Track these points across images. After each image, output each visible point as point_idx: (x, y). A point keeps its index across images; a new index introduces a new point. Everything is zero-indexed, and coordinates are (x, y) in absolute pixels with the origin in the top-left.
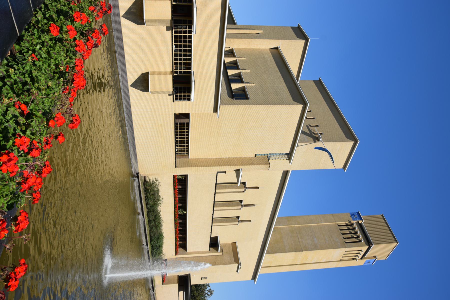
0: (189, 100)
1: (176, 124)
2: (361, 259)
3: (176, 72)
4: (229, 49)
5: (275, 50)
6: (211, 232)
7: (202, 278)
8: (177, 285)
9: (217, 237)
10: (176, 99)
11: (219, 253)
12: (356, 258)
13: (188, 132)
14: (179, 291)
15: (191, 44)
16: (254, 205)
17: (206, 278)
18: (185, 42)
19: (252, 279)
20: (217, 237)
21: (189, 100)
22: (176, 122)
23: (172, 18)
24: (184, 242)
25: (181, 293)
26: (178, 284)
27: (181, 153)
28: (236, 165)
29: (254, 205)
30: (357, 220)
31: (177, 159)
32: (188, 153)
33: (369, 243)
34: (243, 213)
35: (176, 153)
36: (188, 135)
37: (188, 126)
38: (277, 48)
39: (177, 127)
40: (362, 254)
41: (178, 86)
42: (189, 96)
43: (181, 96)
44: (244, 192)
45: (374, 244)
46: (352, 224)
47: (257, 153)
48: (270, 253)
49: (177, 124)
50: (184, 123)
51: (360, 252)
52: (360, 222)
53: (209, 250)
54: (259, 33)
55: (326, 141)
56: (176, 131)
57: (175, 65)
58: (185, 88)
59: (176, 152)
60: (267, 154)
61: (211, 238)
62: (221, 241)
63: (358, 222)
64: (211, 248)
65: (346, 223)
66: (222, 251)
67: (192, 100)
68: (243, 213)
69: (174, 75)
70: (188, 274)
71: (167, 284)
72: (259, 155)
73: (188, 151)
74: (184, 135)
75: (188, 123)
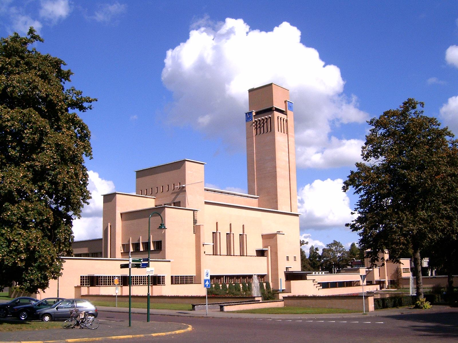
2: (287, 115)
4: (122, 247)
8: (292, 282)
9: (256, 250)
11: (269, 249)
14: (307, 280)
16: (230, 224)
17: (295, 257)
19: (298, 216)
20: (256, 250)
21: (164, 276)
26: (291, 281)
28: (200, 247)
29: (230, 224)
30: (252, 117)
33: (270, 110)
34: (237, 232)
35: (193, 284)
38: (121, 214)
41: (157, 282)
42: (162, 277)
43: (162, 281)
45: (273, 105)
48: (277, 200)
52: (254, 114)
54: (111, 226)
55: (185, 182)
59: (191, 283)
60: (194, 226)
61: (257, 256)
62: (260, 247)
65: (255, 129)
66: (267, 247)
68: (237, 232)
70: (285, 273)
72: (194, 232)
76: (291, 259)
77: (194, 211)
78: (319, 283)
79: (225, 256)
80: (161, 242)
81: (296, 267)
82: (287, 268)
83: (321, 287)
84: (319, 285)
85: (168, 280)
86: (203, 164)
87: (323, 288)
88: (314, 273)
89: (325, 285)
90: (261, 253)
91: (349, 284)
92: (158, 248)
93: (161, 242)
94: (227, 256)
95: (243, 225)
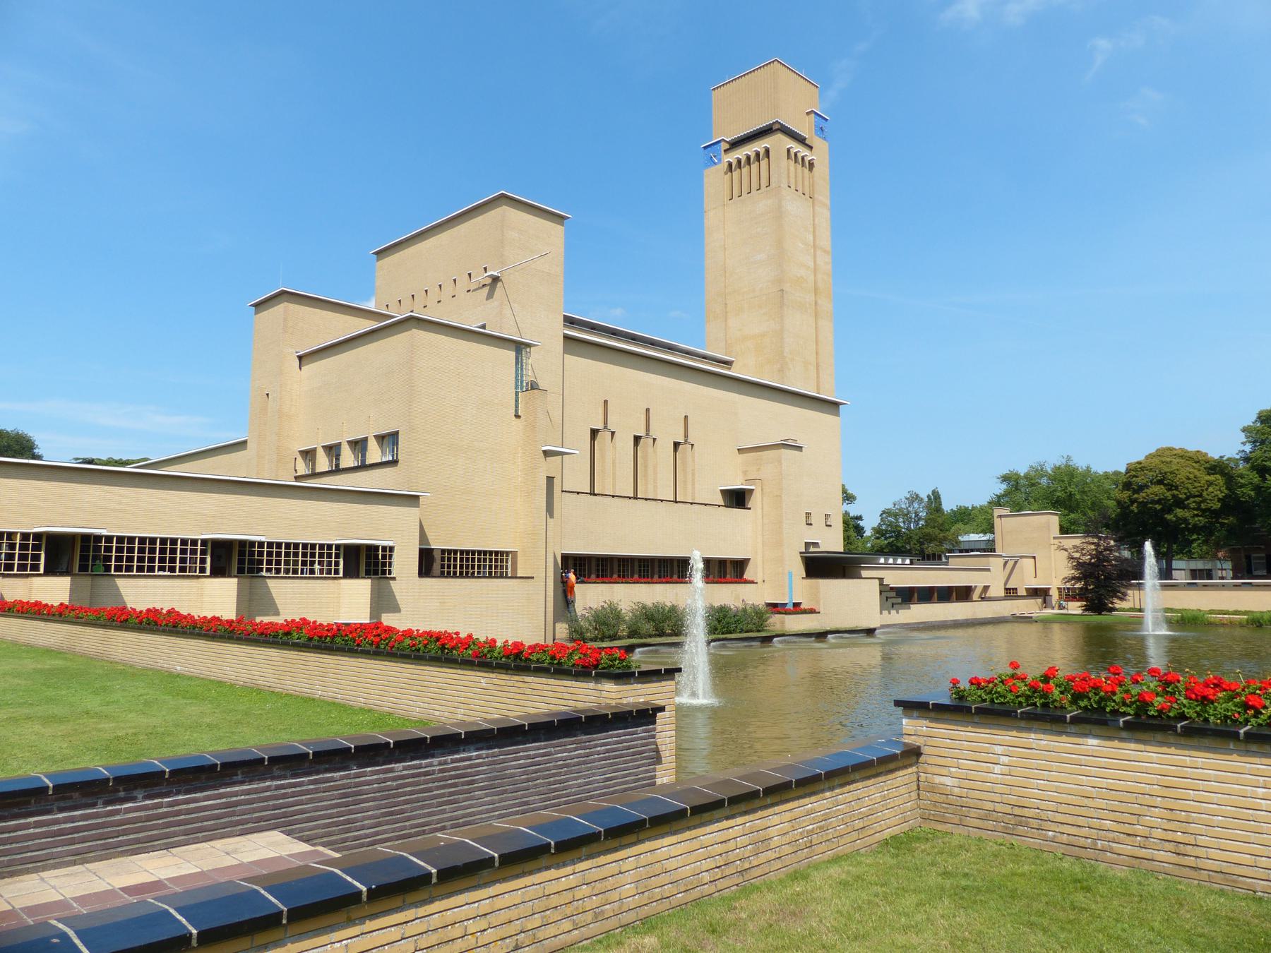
0: (391, 549)
1: (442, 575)
2: (811, 148)
3: (337, 572)
5: (304, 361)
6: (706, 505)
7: (828, 523)
9: (722, 491)
10: (390, 573)
12: (809, 161)
13: (462, 552)
15: (284, 544)
18: (279, 554)
21: (391, 549)
22: (439, 574)
23: (235, 577)
24: (728, 565)
25: (864, 573)
27: (507, 566)
30: (720, 154)
31: (518, 575)
32: (507, 553)
34: (667, 432)
35: (507, 577)
36: (468, 552)
37: (449, 551)
39: (449, 573)
40: (796, 147)
42: (384, 549)
44: (613, 433)
46: (730, 165)
47: (514, 414)
49: (443, 573)
50: (443, 559)
51: (793, 151)
52: (725, 146)
53: (750, 509)
56: (458, 575)
57: (323, 574)
58: (368, 557)
63: (725, 151)
67: (390, 543)
68: (667, 432)
69: (341, 575)
71: (818, 602)
73: (502, 553)
74: (467, 560)
75: (443, 551)
76: (817, 520)
77: (520, 347)
78: (892, 589)
79: (627, 500)
80: (397, 433)
81: (832, 542)
82: (807, 545)
83: (899, 600)
84: (893, 594)
85: (405, 563)
86: (560, 219)
88: (882, 560)
90: (737, 499)
91: (963, 594)
93: (397, 433)
95: (686, 417)
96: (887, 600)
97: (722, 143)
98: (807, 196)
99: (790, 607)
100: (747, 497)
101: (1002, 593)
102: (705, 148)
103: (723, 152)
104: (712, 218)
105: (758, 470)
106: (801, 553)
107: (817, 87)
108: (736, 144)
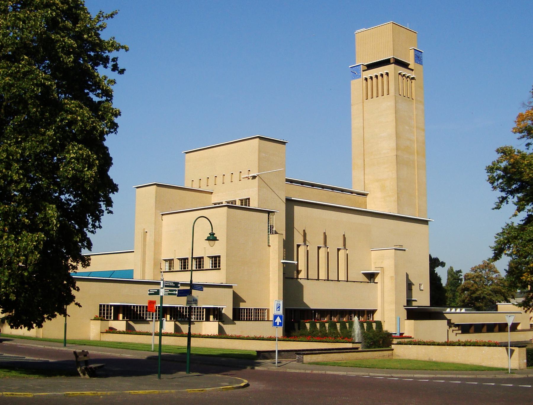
3: (203, 319)
6: (354, 282)
30: (360, 73)
47: (267, 245)
64: (375, 281)
77: (269, 212)
79: (315, 281)
83: (460, 332)
87: (463, 333)
89: (465, 329)
92: (215, 267)
94: (317, 281)
96: (453, 332)
97: (361, 65)
98: (411, 99)
99: (398, 335)
100: (375, 276)
101: (529, 328)
102: (351, 67)
103: (362, 71)
104: (355, 109)
105: (382, 262)
106: (404, 306)
107: (416, 33)
108: (370, 67)
